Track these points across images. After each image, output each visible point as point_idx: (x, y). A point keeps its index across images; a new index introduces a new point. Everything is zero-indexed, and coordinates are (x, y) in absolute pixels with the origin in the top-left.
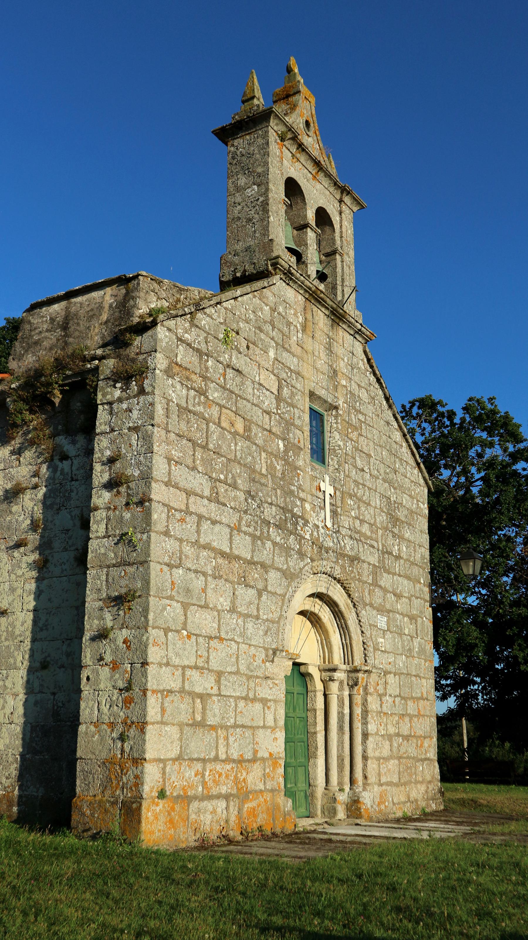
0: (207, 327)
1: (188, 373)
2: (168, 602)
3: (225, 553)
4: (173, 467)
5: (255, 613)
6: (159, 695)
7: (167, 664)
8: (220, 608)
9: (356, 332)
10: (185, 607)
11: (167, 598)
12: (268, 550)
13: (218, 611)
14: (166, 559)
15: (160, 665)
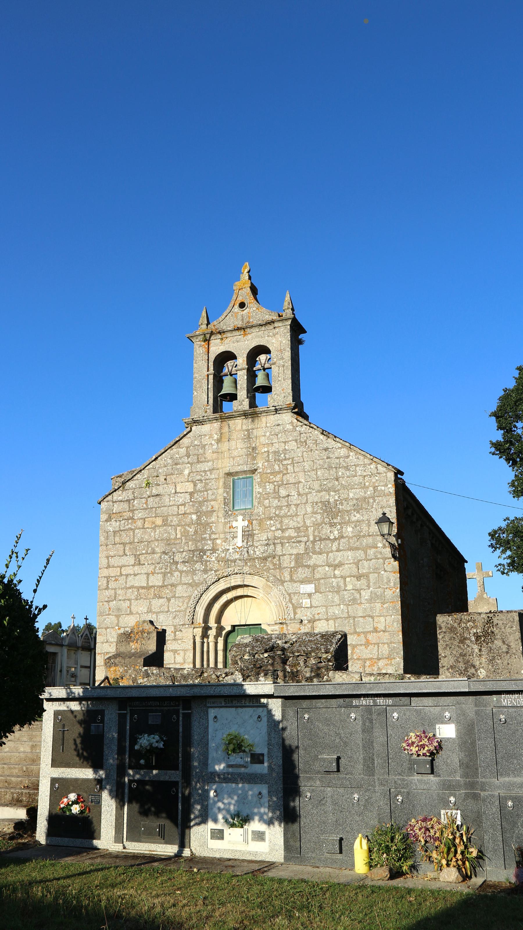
0: (134, 486)
1: (121, 514)
2: (107, 617)
3: (144, 587)
4: (110, 560)
5: (166, 610)
6: (102, 655)
7: (107, 642)
8: (140, 612)
9: (276, 412)
10: (118, 617)
11: (106, 615)
12: (176, 576)
13: (139, 614)
14: (106, 599)
15: (103, 643)
